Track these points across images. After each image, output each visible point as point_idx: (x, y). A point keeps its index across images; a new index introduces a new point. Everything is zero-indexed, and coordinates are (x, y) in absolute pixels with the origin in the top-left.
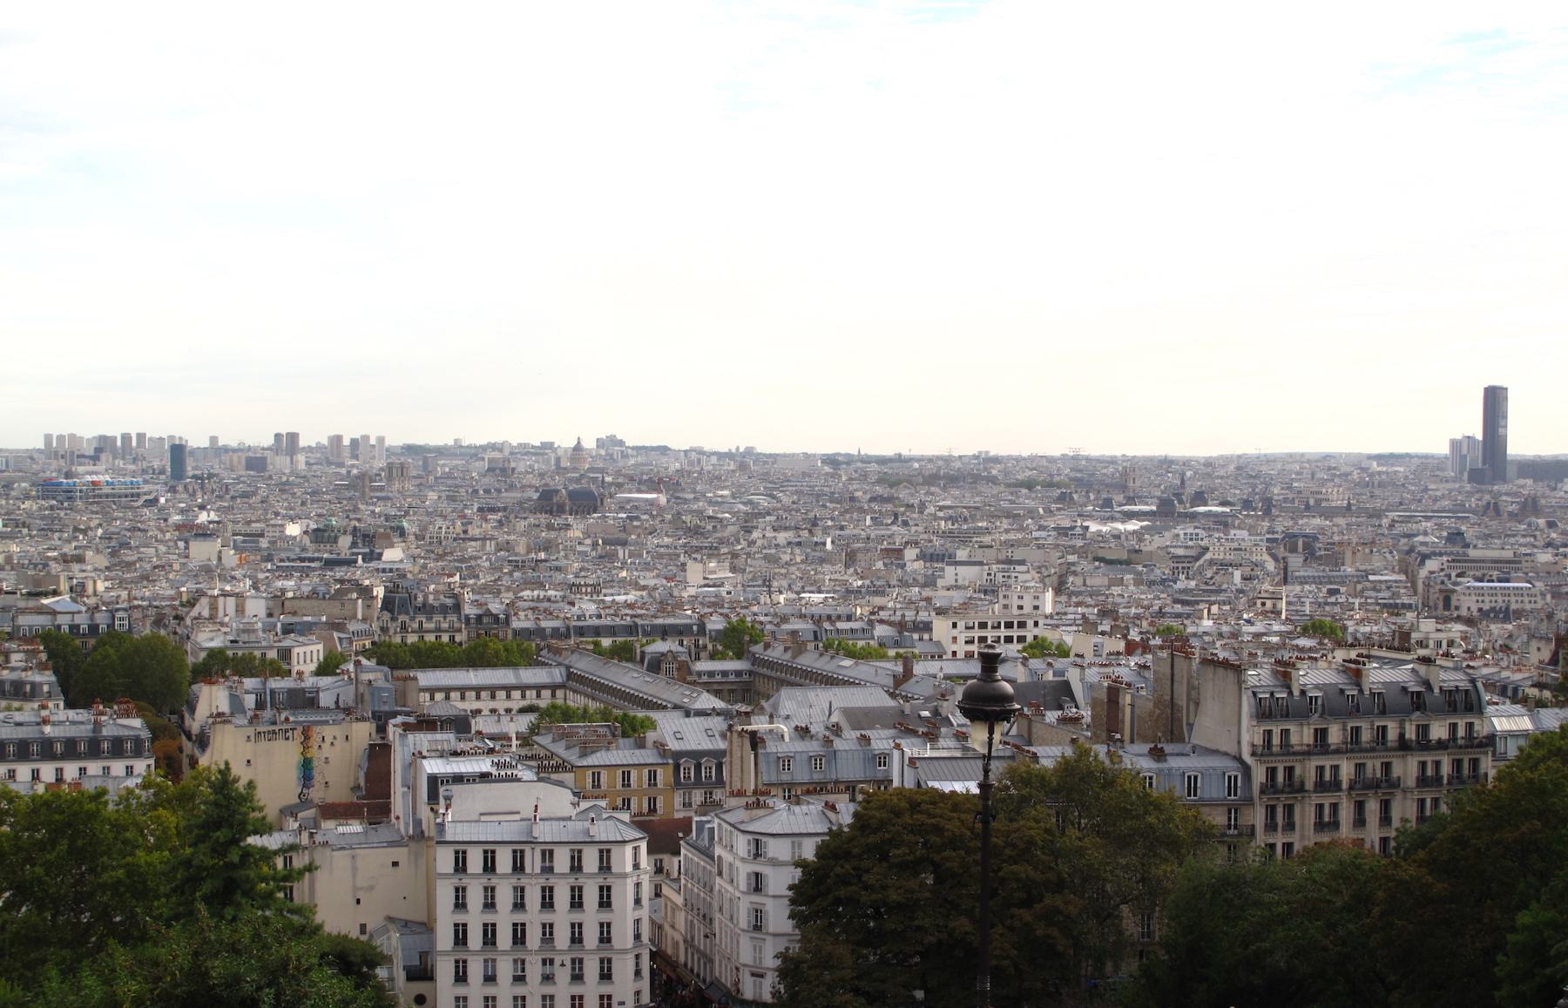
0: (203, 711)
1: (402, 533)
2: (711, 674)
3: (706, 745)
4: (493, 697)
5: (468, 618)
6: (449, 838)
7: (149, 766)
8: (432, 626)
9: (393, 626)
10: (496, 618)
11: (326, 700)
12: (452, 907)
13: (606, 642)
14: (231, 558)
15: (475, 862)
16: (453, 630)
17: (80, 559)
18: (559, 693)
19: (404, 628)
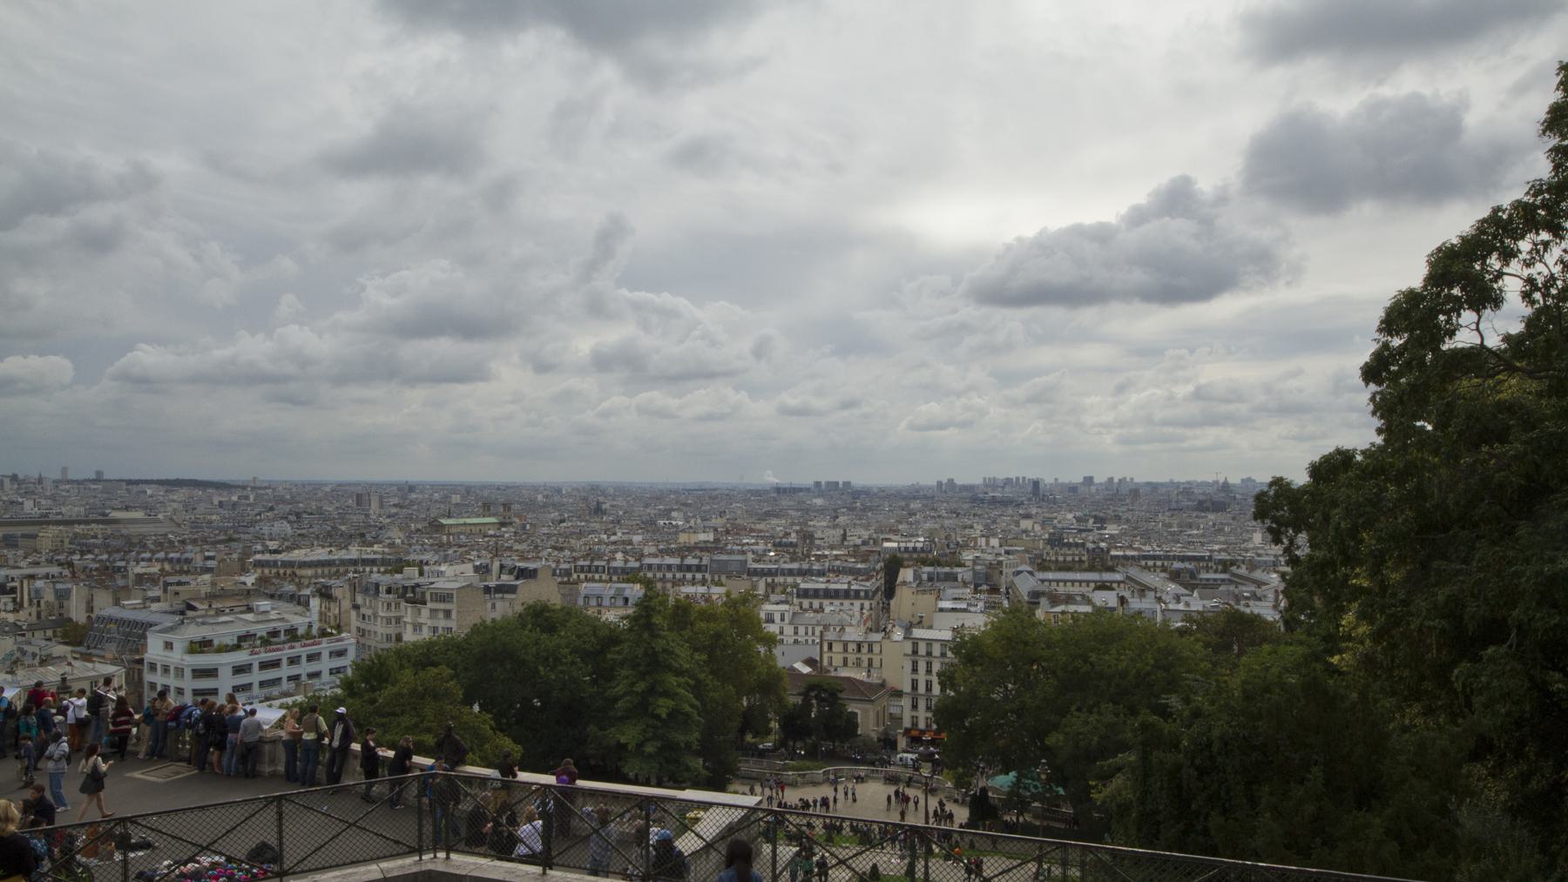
0: (900, 579)
1: (1120, 518)
2: (1208, 580)
3: (1116, 605)
4: (1088, 586)
5: (1088, 550)
6: (912, 636)
7: (871, 604)
8: (1070, 552)
9: (1051, 552)
10: (1102, 549)
11: (959, 579)
12: (910, 671)
13: (1159, 563)
14: (1038, 528)
15: (922, 650)
16: (1081, 555)
17: (972, 527)
18: (1122, 585)
19: (1057, 554)
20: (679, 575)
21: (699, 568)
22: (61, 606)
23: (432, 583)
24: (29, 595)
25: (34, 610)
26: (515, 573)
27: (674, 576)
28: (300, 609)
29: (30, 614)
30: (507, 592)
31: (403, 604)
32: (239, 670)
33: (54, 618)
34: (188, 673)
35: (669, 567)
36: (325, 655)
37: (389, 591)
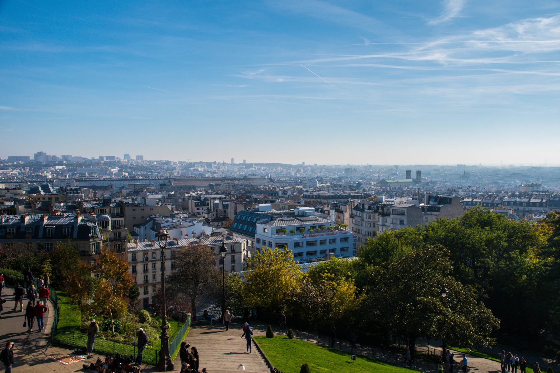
20: (527, 208)
21: (541, 204)
22: (225, 212)
23: (393, 205)
24: (213, 207)
25: (215, 213)
26: (438, 201)
27: (524, 209)
28: (325, 215)
29: (213, 215)
30: (435, 211)
31: (377, 215)
32: (297, 245)
33: (222, 217)
34: (274, 245)
35: (521, 204)
36: (338, 241)
37: (369, 208)
